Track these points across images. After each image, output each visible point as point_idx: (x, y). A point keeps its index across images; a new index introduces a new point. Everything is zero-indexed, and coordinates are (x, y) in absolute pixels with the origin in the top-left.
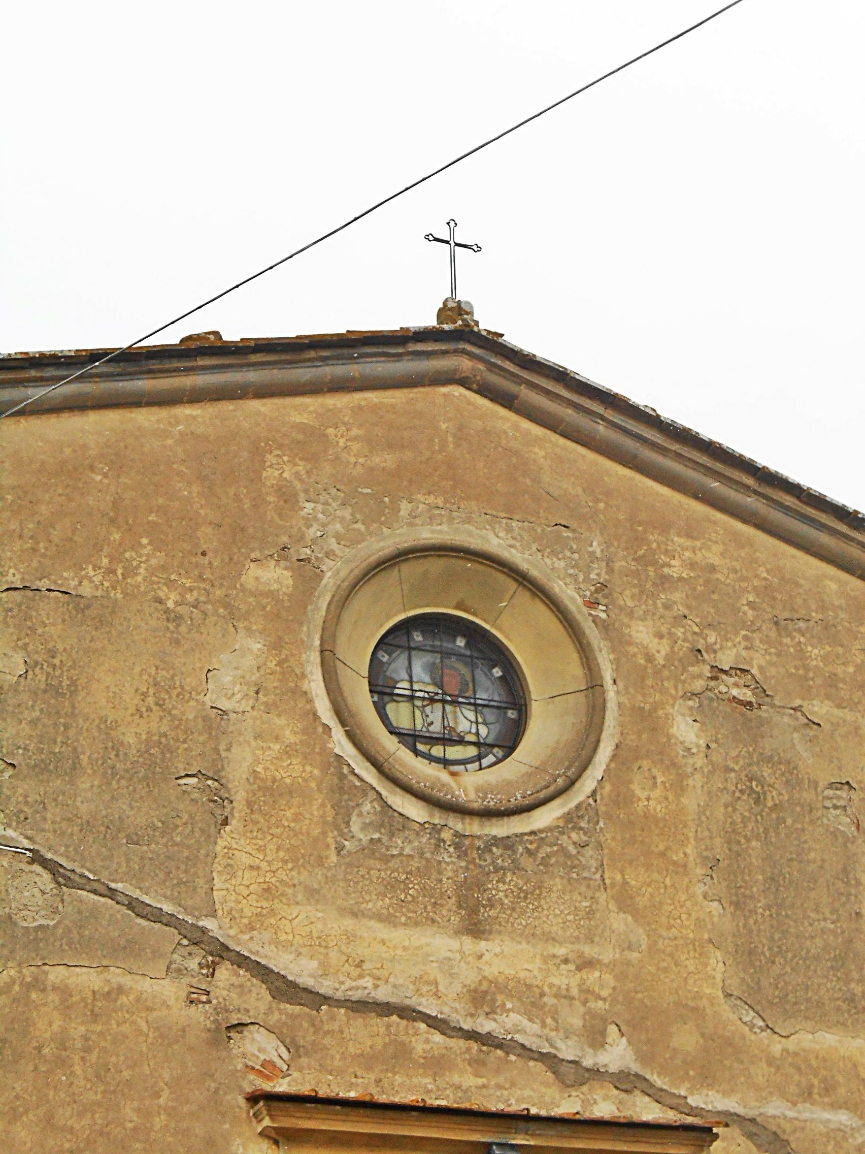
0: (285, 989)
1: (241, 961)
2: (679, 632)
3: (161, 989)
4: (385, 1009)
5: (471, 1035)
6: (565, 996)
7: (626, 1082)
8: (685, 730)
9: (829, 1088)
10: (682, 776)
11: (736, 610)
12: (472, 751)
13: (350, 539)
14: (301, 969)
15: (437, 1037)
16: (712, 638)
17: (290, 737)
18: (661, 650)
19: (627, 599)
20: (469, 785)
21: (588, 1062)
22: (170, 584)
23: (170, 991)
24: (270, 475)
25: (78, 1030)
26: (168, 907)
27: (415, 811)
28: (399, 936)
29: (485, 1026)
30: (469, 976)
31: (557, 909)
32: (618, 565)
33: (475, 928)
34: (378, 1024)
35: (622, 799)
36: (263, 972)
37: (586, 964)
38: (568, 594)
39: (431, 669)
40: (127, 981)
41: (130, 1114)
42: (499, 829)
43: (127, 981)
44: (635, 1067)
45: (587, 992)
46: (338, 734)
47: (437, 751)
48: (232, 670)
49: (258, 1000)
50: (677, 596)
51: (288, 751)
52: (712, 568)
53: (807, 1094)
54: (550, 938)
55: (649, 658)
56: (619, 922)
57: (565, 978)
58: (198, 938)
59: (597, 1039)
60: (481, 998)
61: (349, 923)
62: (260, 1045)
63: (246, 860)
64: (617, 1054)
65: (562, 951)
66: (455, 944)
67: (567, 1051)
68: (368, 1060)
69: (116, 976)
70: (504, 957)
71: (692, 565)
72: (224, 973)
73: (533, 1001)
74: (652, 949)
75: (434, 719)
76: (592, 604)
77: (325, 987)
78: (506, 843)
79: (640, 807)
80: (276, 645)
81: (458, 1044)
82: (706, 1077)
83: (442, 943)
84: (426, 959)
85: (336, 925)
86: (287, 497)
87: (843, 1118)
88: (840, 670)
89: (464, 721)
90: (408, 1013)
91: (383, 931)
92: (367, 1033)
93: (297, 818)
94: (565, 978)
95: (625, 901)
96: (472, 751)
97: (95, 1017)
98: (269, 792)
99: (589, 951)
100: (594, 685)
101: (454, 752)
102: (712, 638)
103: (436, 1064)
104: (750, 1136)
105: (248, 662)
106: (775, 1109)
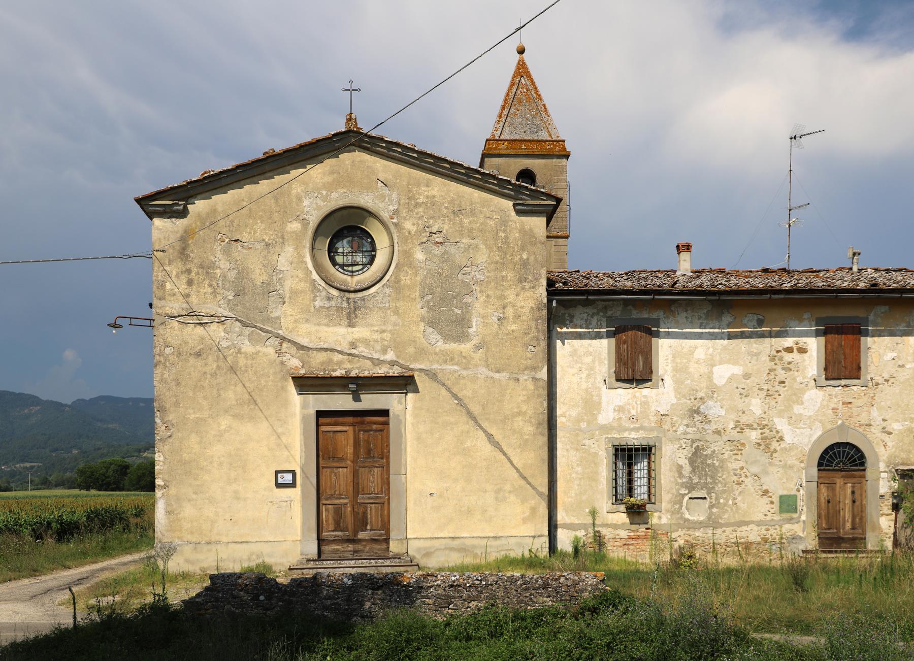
0: (300, 347)
1: (289, 341)
2: (420, 222)
3: (269, 350)
4: (327, 350)
5: (350, 355)
6: (376, 341)
7: (392, 363)
8: (419, 256)
9: (452, 359)
10: (417, 271)
11: (440, 210)
12: (361, 267)
13: (318, 208)
14: (304, 342)
15: (340, 356)
16: (431, 222)
17: (301, 276)
18: (413, 229)
19: (404, 213)
20: (353, 282)
21: (382, 359)
22: (266, 234)
23: (271, 351)
24: (294, 192)
25: (249, 362)
26: (270, 329)
27: (335, 293)
28: (331, 329)
29: (354, 351)
30: (350, 338)
31: (375, 318)
32: (402, 201)
33: (351, 325)
34: (324, 354)
35: (398, 281)
36: (295, 343)
37: (384, 331)
38: (385, 215)
39: (348, 242)
40: (261, 349)
41: (263, 382)
42: (360, 295)
43: (261, 349)
44: (395, 359)
45: (383, 339)
46: (314, 273)
47: (350, 269)
48: (285, 258)
49: (294, 350)
50: (421, 209)
51: (300, 280)
52: (434, 197)
53: (445, 362)
54: (372, 325)
55: (410, 233)
56: (394, 318)
57: (376, 336)
58: (277, 336)
59: (384, 351)
60: (353, 345)
61: (317, 328)
62: (294, 363)
63: (289, 313)
64: (390, 356)
65: (376, 329)
66: (346, 330)
67: (376, 356)
68: (322, 363)
69: (258, 348)
70: (359, 332)
71: (427, 197)
72: (285, 345)
73: (366, 342)
74: (403, 325)
75: (349, 259)
76: (392, 218)
77: (310, 346)
78: (363, 299)
79: (402, 283)
80: (296, 248)
81: (346, 357)
82: (415, 360)
83: (342, 330)
84: (338, 335)
85: (314, 328)
86: (299, 199)
87: (456, 367)
88: (474, 226)
89: (359, 258)
90: (332, 350)
91: (326, 329)
92: (321, 357)
93: (303, 299)
94: (376, 336)
95: (396, 312)
96: (361, 267)
97: (253, 359)
98: (294, 293)
99: (384, 328)
100: (392, 246)
101: (355, 268)
102: (431, 222)
103: (339, 363)
104: (427, 375)
105: (289, 255)
106: (435, 366)
